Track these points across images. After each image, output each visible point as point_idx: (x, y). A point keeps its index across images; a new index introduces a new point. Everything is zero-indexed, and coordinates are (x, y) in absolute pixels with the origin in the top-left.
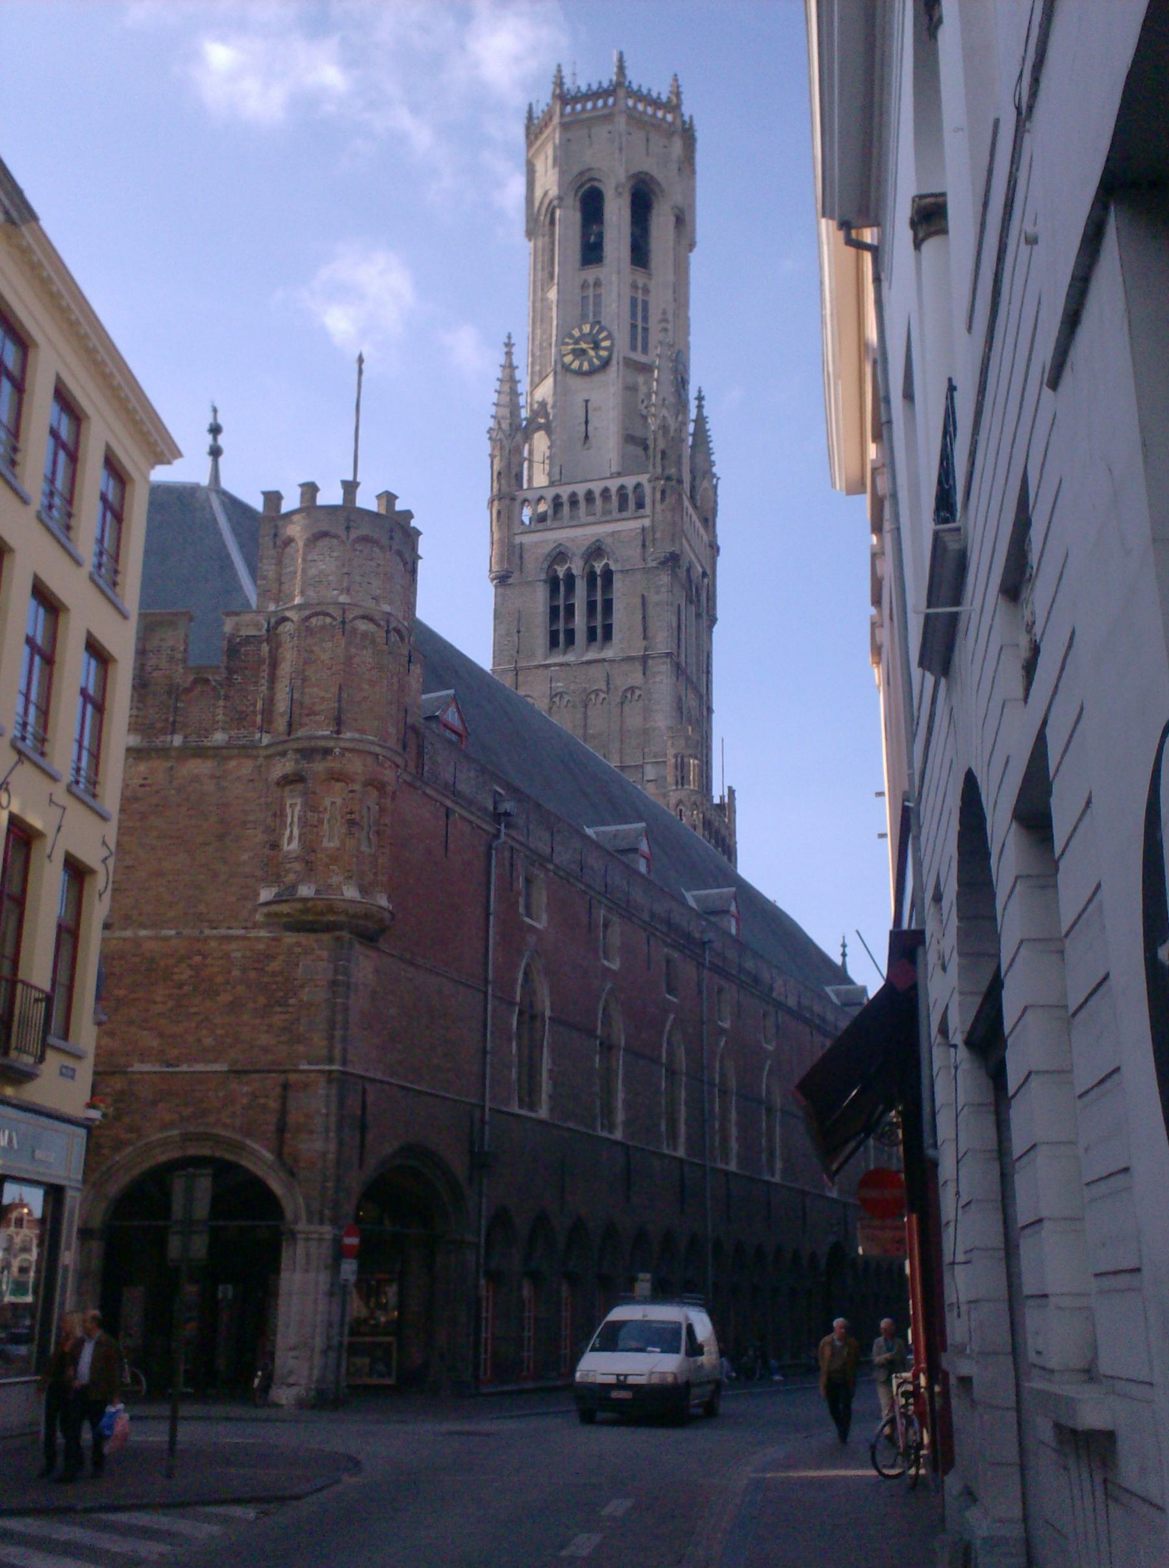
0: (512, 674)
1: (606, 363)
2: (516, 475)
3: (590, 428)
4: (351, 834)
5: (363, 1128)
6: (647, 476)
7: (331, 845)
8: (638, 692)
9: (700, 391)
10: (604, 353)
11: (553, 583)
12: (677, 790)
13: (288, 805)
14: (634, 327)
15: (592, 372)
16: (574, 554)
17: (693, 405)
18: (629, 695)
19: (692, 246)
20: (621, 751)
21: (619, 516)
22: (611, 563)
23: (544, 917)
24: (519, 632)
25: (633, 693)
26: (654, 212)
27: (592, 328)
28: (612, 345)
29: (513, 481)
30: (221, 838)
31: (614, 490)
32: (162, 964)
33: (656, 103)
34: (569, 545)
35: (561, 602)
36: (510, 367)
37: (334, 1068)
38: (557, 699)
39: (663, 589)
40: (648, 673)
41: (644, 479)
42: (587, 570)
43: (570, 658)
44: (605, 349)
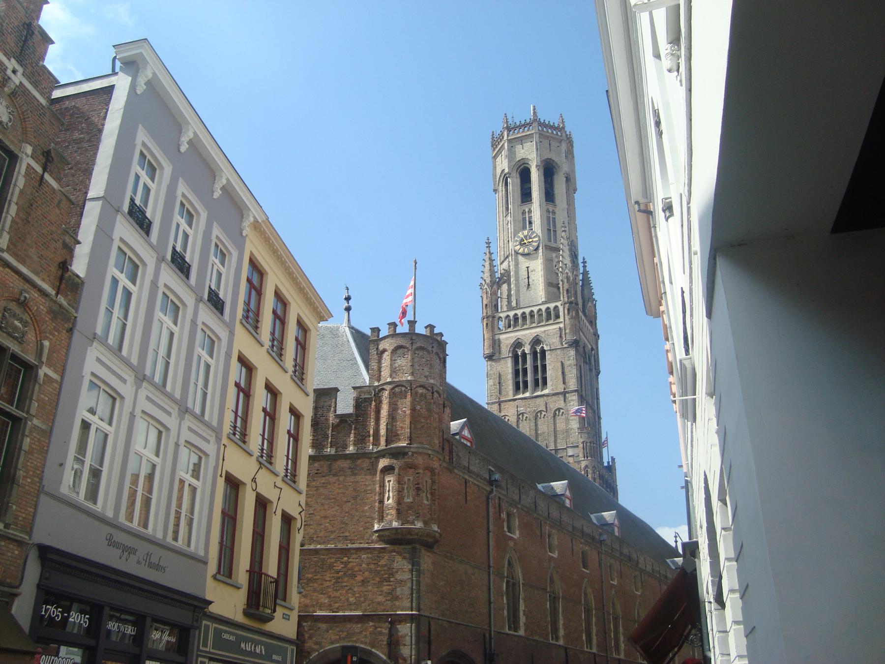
0: (497, 405)
1: (537, 249)
2: (495, 305)
4: (418, 495)
5: (429, 643)
7: (409, 500)
8: (562, 411)
9: (584, 259)
11: (515, 358)
12: (584, 460)
13: (387, 480)
14: (549, 230)
16: (526, 343)
17: (581, 265)
19: (575, 190)
20: (555, 442)
22: (545, 346)
23: (517, 532)
26: (555, 177)
29: (493, 308)
30: (355, 498)
31: (544, 310)
32: (328, 561)
33: (553, 127)
37: (414, 612)
38: (521, 416)
39: (572, 358)
40: (567, 400)
41: (559, 304)
43: (527, 395)
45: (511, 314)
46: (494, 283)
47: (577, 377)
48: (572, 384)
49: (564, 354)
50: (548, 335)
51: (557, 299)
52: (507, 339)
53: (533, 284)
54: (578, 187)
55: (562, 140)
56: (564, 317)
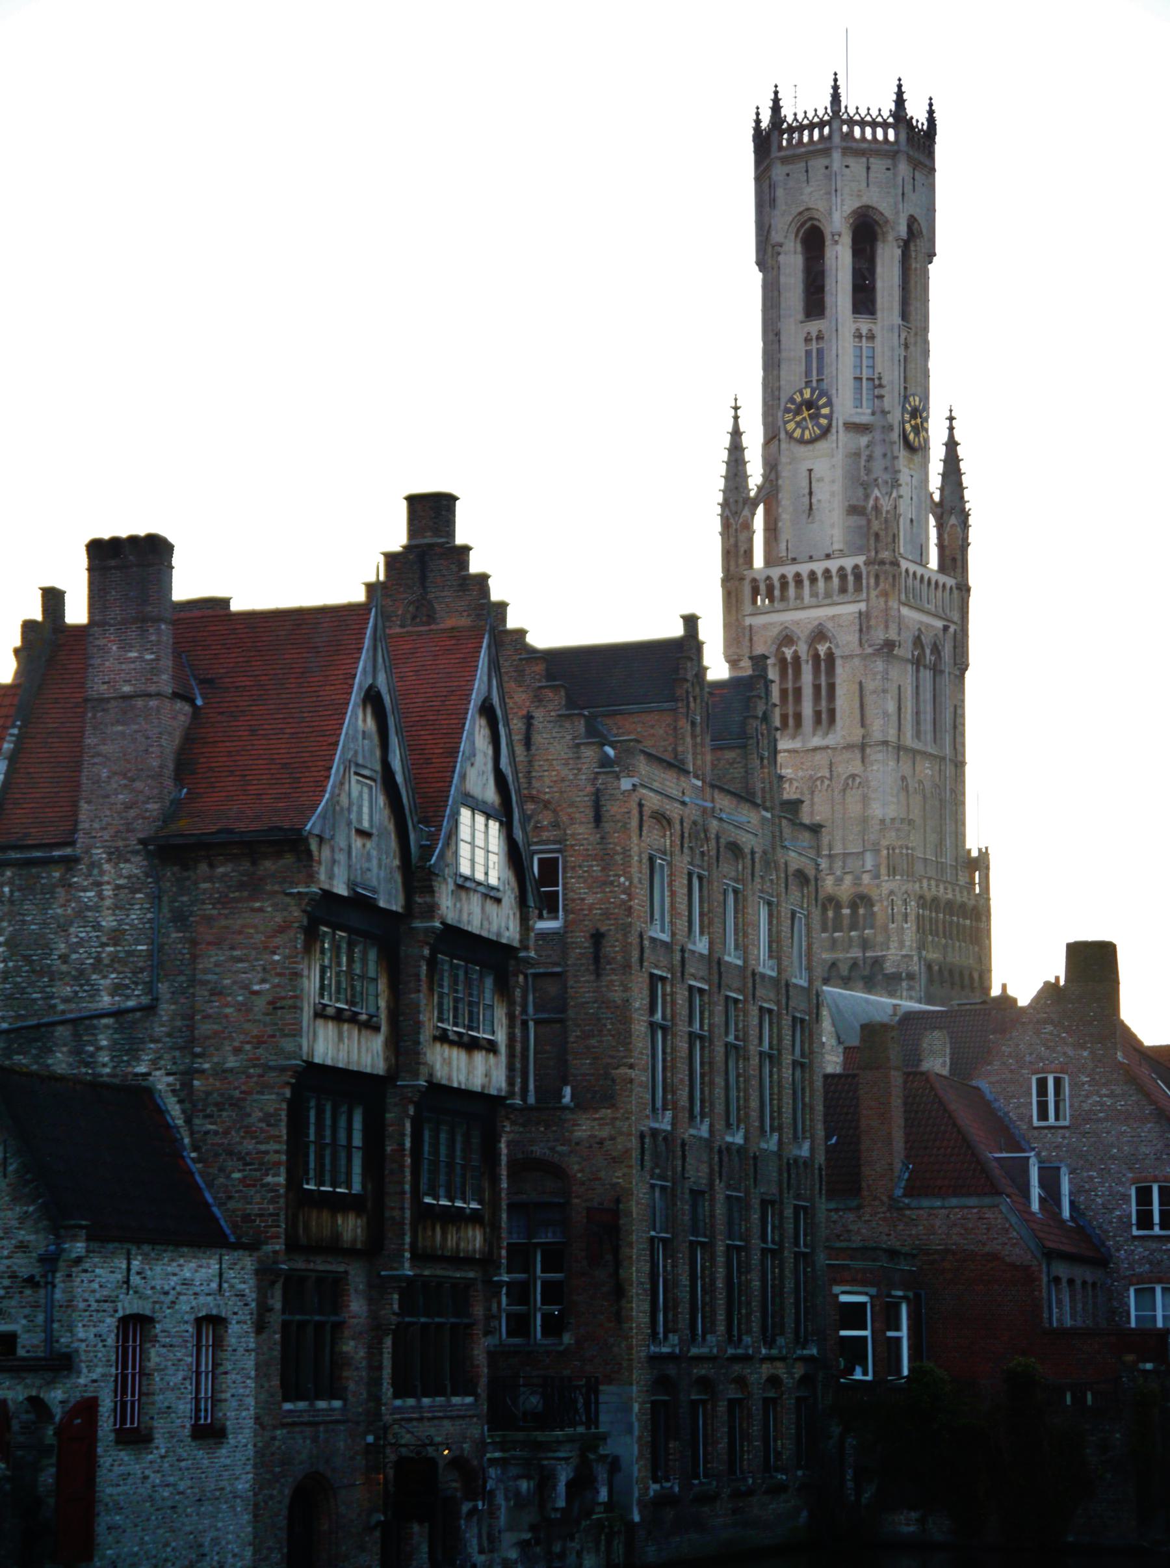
1: (826, 432)
2: (745, 552)
3: (814, 500)
8: (858, 780)
10: (824, 421)
14: (858, 379)
15: (812, 441)
16: (799, 638)
18: (850, 782)
20: (844, 839)
21: (836, 598)
25: (854, 779)
27: (812, 393)
28: (832, 412)
29: (741, 561)
31: (834, 571)
34: (794, 628)
35: (790, 685)
36: (736, 434)
39: (879, 677)
40: (866, 760)
41: (860, 560)
42: (811, 653)
44: (825, 416)
45: (775, 573)
46: (745, 503)
49: (865, 666)
50: (839, 625)
51: (858, 551)
52: (765, 627)
53: (818, 509)
54: (938, 249)
55: (897, 152)
56: (868, 594)
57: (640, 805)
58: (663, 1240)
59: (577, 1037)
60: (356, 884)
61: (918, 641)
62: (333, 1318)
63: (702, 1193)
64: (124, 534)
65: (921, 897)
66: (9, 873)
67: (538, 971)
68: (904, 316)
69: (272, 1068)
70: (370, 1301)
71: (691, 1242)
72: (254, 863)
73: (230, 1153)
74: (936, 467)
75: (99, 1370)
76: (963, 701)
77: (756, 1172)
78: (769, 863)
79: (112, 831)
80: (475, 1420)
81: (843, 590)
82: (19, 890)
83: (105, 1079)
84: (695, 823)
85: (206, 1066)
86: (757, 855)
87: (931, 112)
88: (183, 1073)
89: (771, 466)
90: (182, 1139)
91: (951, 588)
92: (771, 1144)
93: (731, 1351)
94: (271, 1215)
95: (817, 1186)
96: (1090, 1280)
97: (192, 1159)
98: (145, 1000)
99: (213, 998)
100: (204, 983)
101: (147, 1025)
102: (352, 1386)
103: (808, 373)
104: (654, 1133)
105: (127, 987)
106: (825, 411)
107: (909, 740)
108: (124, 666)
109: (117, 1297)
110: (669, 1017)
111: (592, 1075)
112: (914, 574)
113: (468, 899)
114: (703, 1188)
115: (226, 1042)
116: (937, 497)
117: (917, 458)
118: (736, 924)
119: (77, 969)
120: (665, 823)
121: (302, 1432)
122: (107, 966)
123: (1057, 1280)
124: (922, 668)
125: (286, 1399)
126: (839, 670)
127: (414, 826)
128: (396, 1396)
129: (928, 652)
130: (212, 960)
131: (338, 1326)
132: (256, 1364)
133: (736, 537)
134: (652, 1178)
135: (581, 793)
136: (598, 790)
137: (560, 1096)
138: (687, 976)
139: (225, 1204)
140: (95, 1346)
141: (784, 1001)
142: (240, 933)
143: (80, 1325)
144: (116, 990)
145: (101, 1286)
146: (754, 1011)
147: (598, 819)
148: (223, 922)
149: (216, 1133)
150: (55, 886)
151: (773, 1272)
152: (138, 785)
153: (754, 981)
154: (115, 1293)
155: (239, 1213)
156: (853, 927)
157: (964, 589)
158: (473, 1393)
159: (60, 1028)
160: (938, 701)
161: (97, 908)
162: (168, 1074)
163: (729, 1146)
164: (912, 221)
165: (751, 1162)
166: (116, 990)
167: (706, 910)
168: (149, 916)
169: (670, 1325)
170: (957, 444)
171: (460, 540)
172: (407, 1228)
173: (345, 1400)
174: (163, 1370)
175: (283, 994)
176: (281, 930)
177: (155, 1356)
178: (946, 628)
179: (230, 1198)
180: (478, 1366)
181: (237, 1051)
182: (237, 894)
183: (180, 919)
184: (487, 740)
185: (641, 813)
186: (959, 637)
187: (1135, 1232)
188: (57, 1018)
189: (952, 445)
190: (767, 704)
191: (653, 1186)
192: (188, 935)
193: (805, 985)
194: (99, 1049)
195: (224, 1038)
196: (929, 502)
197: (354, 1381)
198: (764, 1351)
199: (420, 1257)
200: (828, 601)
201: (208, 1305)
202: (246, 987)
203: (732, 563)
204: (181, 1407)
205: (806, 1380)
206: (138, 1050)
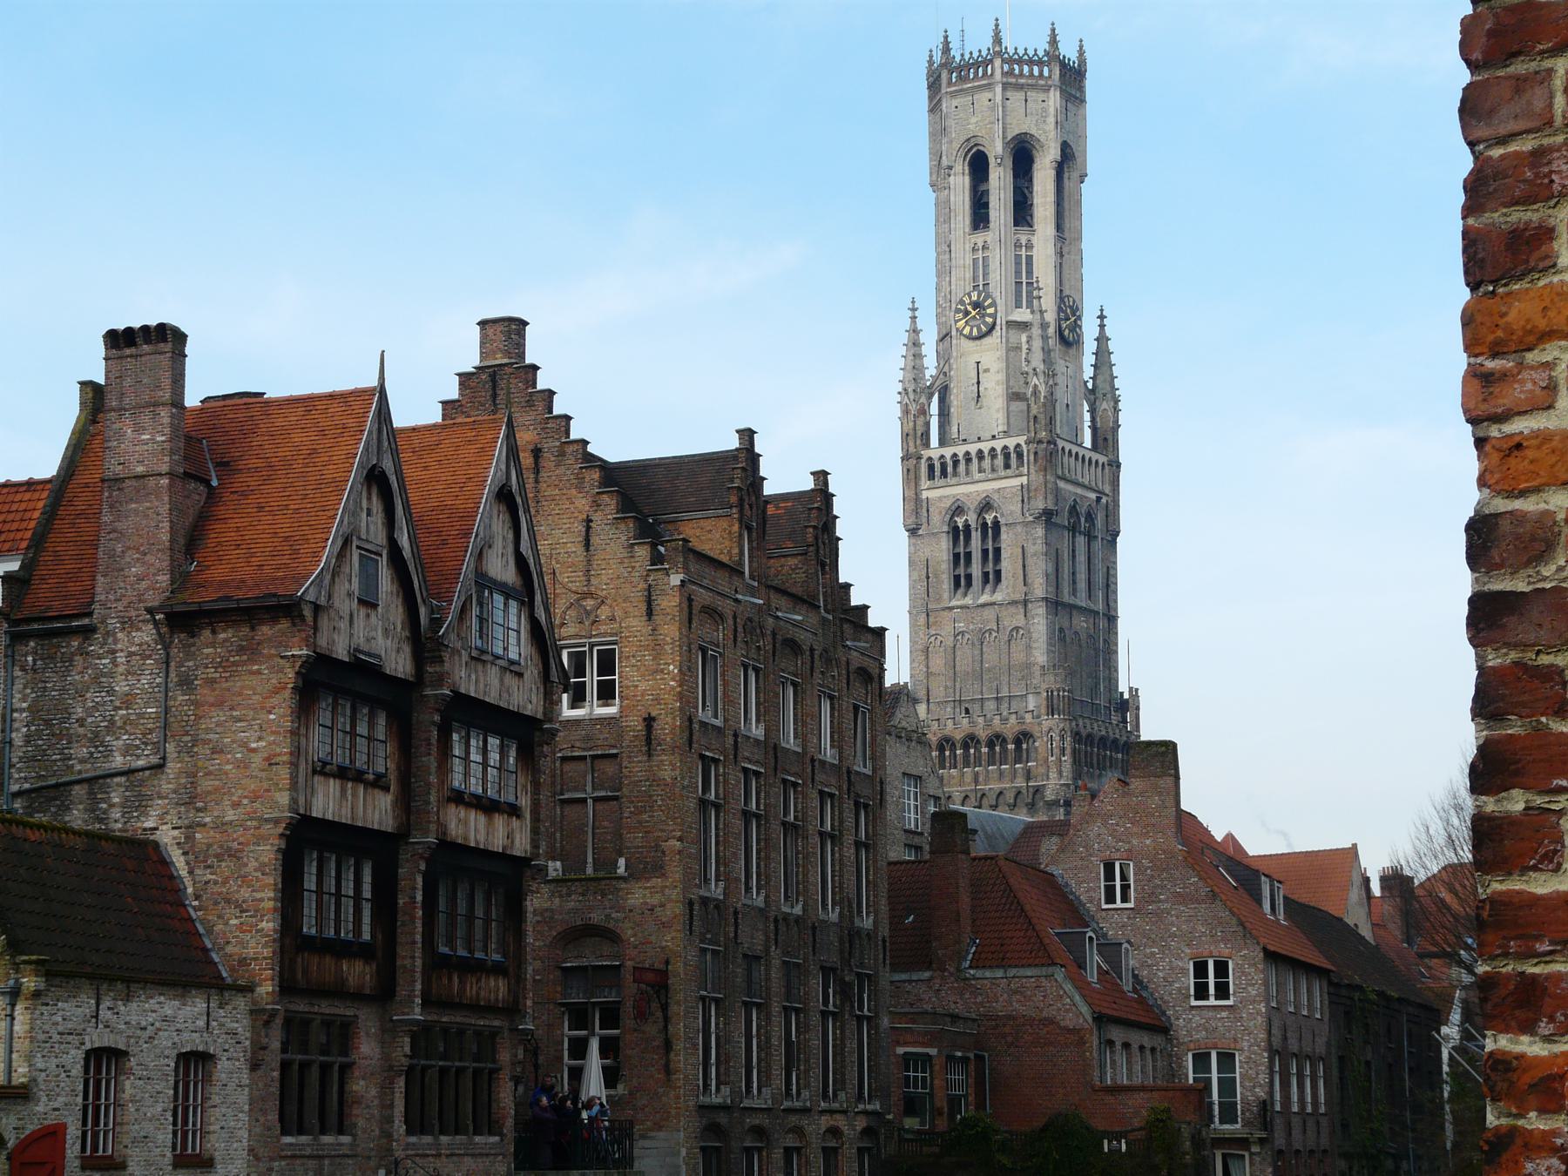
0: (924, 615)
1: (992, 328)
6: (1025, 438)
8: (1021, 632)
11: (955, 531)
14: (1019, 284)
21: (1003, 474)
24: (928, 578)
26: (1035, 166)
27: (979, 297)
28: (996, 311)
29: (919, 442)
35: (962, 550)
38: (960, 637)
39: (1039, 541)
41: (1021, 440)
42: (980, 521)
43: (968, 601)
44: (990, 315)
45: (948, 452)
47: (1047, 575)
48: (1039, 588)
52: (940, 499)
57: (690, 600)
58: (717, 1001)
59: (631, 812)
60: (357, 650)
61: (1073, 510)
62: (344, 1059)
63: (758, 958)
64: (137, 324)
65: (1078, 733)
66: (32, 644)
67: (595, 753)
68: (1059, 227)
69: (266, 820)
70: (382, 1043)
71: (745, 1003)
72: (253, 629)
73: (228, 901)
74: (1088, 359)
75: (61, 1099)
76: (1115, 563)
77: (814, 940)
78: (828, 661)
79: (125, 602)
80: (500, 1157)
81: (1007, 466)
82: (41, 659)
83: (118, 834)
84: (750, 620)
85: (208, 820)
86: (817, 653)
87: (1081, 52)
88: (188, 827)
89: (944, 357)
90: (186, 888)
91: (1103, 464)
92: (834, 916)
93: (787, 1104)
94: (265, 958)
95: (881, 956)
96: (1148, 1045)
97: (194, 908)
98: (154, 760)
99: (215, 756)
100: (206, 742)
101: (156, 782)
102: (361, 1123)
103: (974, 280)
104: (705, 901)
105: (138, 747)
106: (990, 311)
107: (1066, 597)
108: (137, 448)
109: (84, 1030)
110: (722, 796)
111: (642, 847)
112: (1070, 451)
113: (485, 672)
114: (758, 953)
115: (225, 797)
116: (1090, 385)
117: (1072, 351)
118: (795, 715)
119: (93, 732)
120: (718, 618)
121: (303, 1164)
122: (120, 728)
123: (1111, 1043)
124: (1077, 534)
125: (285, 1132)
126: (1004, 536)
127: (424, 601)
128: (409, 1132)
129: (1083, 520)
130: (213, 720)
131: (345, 1069)
132: (251, 1099)
133: (915, 421)
134: (702, 941)
135: (634, 590)
136: (650, 586)
137: (616, 867)
138: (739, 759)
139: (223, 949)
140: (58, 1076)
141: (845, 787)
142: (240, 694)
143: (39, 1055)
144: (127, 750)
145: (64, 1019)
146: (815, 795)
147: (650, 613)
148: (225, 685)
149: (216, 883)
150: (73, 654)
151: (834, 1033)
152: (149, 558)
153: (813, 766)
154: (82, 1026)
155: (236, 957)
156: (1018, 760)
157: (1115, 465)
158: (501, 1135)
159: (77, 787)
160: (1092, 561)
161: (111, 675)
162: (173, 828)
163: (786, 917)
164: (1065, 148)
165: (810, 932)
166: (127, 750)
167: (762, 700)
168: (158, 680)
169: (722, 1078)
170: (1108, 339)
171: (528, 361)
172: (418, 975)
173: (354, 1136)
174: (140, 1101)
175: (278, 750)
176: (277, 691)
177: (129, 1087)
178: (1099, 499)
179: (228, 943)
180: (504, 1108)
181: (236, 805)
182: (237, 658)
183: (186, 683)
184: (508, 525)
185: (690, 607)
186: (1111, 508)
187: (1194, 1003)
188: (73, 778)
189: (1102, 339)
190: (828, 515)
191: (704, 951)
192: (193, 697)
193: (870, 773)
194: (112, 806)
195: (224, 794)
196: (1083, 390)
197: (364, 1119)
198: (822, 1104)
199: (426, 1003)
200: (995, 476)
201: (193, 1042)
202: (244, 745)
203: (911, 444)
204: (161, 1137)
205: (867, 1132)
206: (146, 806)
